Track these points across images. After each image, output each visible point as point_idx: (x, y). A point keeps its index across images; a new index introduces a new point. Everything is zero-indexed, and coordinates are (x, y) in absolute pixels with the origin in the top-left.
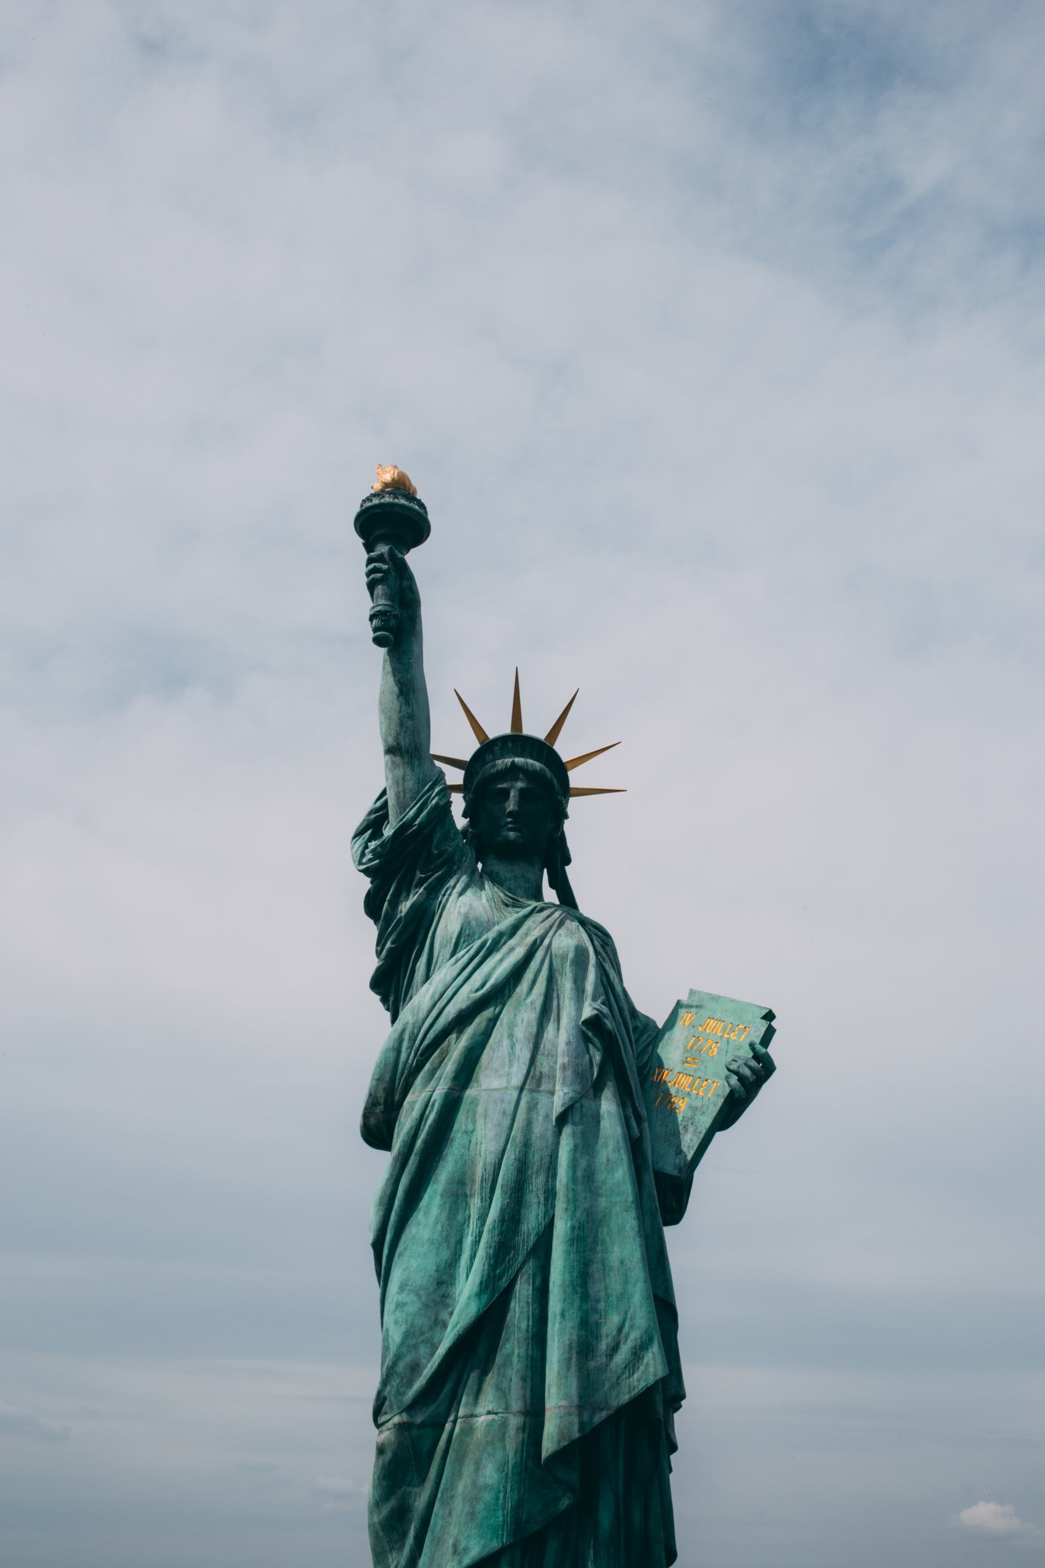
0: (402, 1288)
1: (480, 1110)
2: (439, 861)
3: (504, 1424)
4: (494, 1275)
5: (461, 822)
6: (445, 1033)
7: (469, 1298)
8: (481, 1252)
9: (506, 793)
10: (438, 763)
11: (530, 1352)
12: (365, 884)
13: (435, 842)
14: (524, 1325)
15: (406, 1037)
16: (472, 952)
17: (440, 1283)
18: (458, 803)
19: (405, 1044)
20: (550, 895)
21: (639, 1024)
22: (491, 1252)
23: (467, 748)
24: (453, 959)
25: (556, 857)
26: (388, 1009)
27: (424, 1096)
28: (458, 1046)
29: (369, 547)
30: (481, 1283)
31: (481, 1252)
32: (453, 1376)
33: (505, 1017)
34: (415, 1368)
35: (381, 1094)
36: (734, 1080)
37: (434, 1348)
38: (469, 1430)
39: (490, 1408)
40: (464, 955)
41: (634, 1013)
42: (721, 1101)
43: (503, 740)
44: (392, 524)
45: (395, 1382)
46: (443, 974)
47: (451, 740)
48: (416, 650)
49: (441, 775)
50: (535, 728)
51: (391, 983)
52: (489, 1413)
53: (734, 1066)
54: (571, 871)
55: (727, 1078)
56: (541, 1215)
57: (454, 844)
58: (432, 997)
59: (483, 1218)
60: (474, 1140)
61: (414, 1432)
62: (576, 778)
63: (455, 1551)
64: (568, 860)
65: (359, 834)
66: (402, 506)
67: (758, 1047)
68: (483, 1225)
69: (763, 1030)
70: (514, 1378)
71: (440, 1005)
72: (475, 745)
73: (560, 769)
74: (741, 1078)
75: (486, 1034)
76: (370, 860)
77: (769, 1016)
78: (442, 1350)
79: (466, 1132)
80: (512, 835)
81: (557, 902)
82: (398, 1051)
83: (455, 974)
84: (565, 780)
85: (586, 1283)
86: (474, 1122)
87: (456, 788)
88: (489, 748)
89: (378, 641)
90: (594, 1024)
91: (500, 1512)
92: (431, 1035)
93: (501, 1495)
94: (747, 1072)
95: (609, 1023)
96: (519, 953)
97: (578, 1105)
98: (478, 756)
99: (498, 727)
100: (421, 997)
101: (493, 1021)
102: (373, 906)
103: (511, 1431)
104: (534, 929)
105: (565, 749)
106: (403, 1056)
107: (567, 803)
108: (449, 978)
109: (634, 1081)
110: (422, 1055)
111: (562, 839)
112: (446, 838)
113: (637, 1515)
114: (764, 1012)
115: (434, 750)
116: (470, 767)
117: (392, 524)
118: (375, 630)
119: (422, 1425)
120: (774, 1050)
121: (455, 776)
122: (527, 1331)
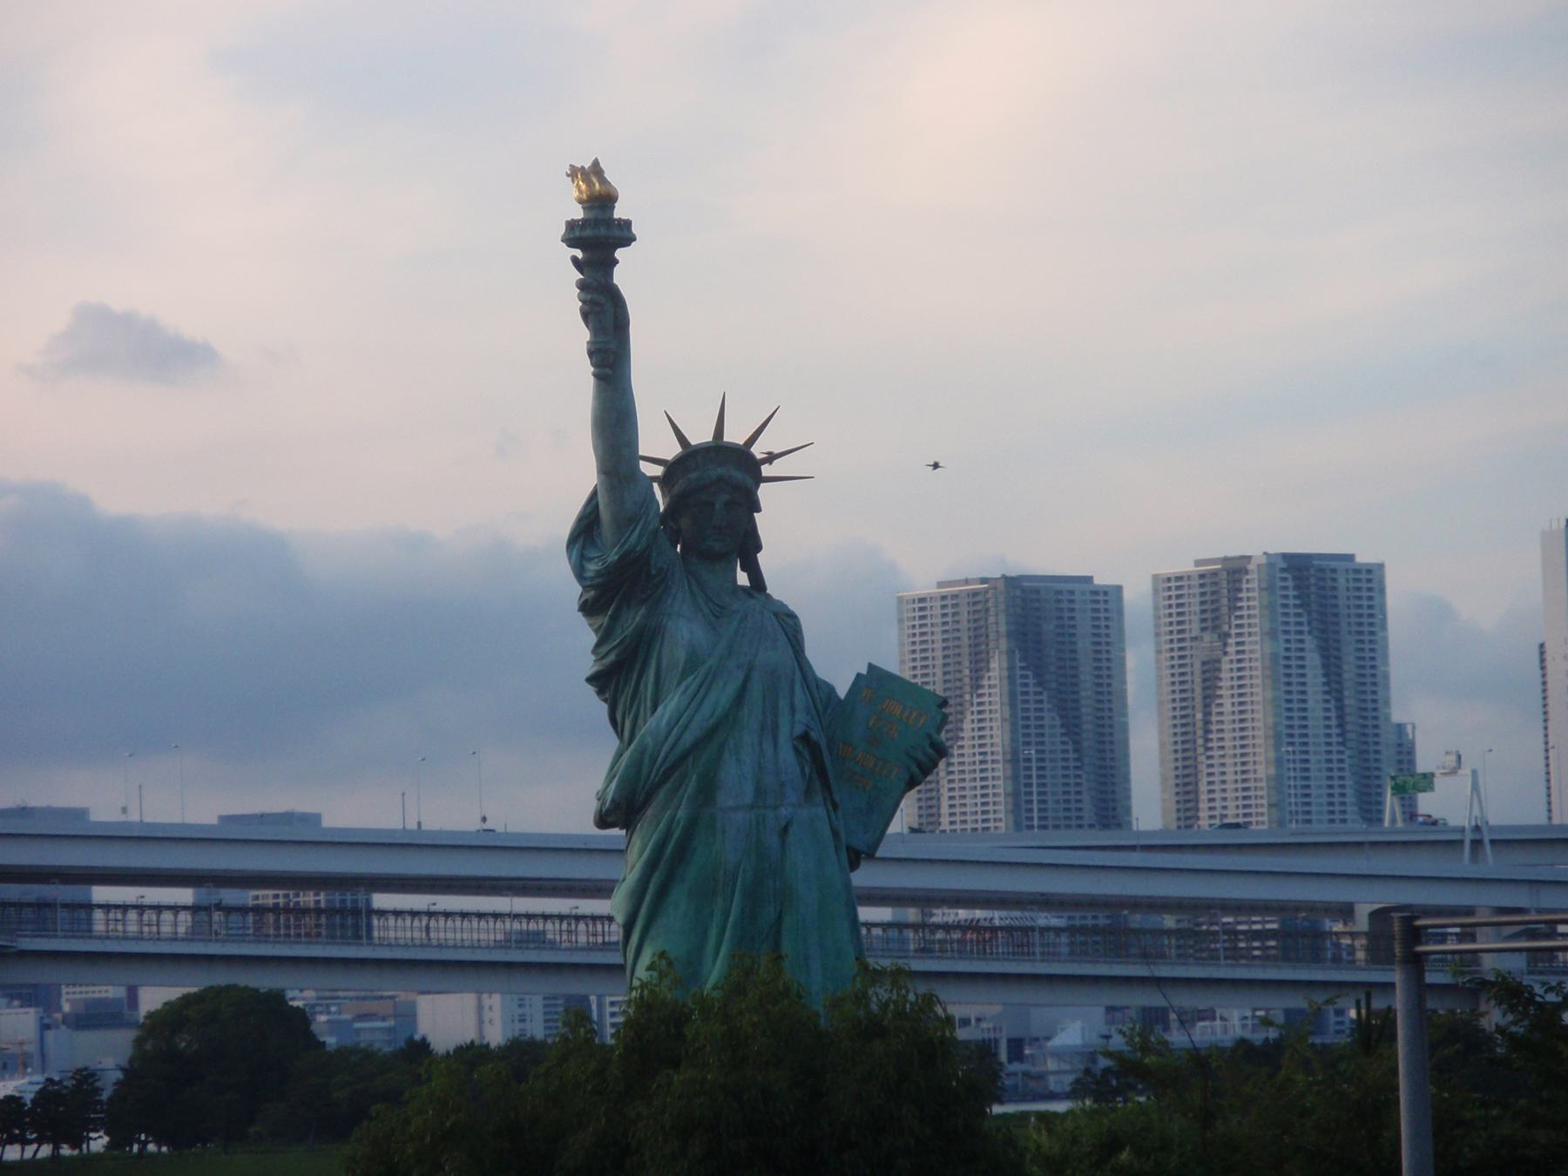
6: (684, 757)
20: (742, 579)
23: (672, 450)
24: (682, 687)
25: (748, 546)
26: (605, 701)
44: (598, 237)
59: (726, 914)
64: (759, 548)
87: (654, 479)
88: (691, 457)
90: (805, 738)
92: (672, 758)
95: (813, 735)
106: (644, 772)
116: (674, 469)
117: (598, 237)
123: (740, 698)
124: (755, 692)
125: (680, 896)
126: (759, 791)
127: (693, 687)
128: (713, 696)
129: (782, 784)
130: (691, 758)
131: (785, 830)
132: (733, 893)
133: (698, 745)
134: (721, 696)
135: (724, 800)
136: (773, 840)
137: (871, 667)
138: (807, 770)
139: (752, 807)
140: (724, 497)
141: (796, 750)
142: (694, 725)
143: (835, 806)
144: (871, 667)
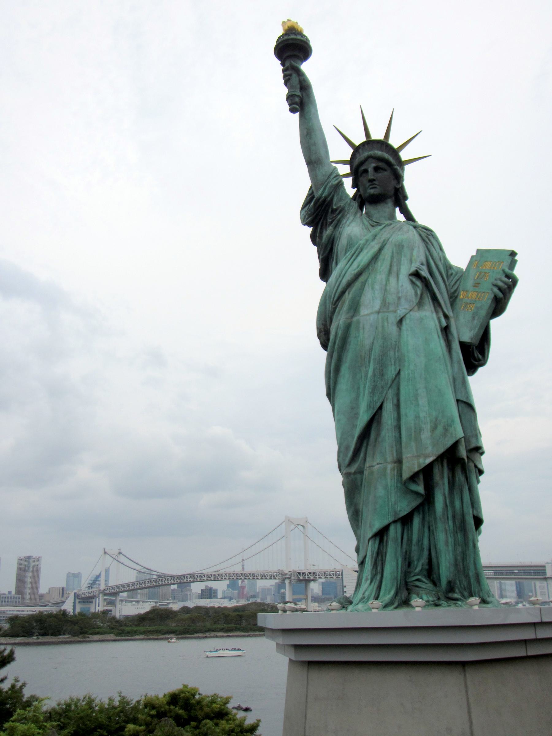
0: (338, 413)
1: (361, 325)
2: (337, 212)
3: (385, 469)
4: (373, 401)
5: (351, 192)
6: (343, 293)
7: (363, 413)
8: (367, 392)
9: (366, 171)
10: (334, 165)
11: (394, 434)
12: (310, 230)
13: (334, 202)
14: (389, 422)
15: (327, 298)
16: (353, 252)
17: (353, 408)
18: (348, 183)
19: (328, 302)
20: (400, 217)
21: (453, 272)
22: (371, 390)
23: (347, 153)
25: (399, 198)
27: (337, 323)
28: (348, 297)
29: (283, 64)
30: (367, 406)
31: (367, 392)
32: (363, 449)
33: (370, 280)
34: (347, 448)
35: (322, 327)
36: (496, 290)
37: (353, 437)
38: (372, 473)
39: (378, 461)
40: (349, 254)
41: (448, 267)
42: (490, 301)
43: (363, 144)
45: (341, 456)
46: (341, 265)
47: (339, 152)
48: (313, 110)
49: (335, 168)
50: (377, 135)
51: (325, 274)
52: (378, 464)
53: (495, 282)
54: (408, 203)
55: (492, 290)
56: (393, 370)
57: (344, 202)
58: (336, 277)
59: (366, 375)
60: (359, 340)
61: (352, 476)
62: (404, 155)
63: (370, 527)
64: (406, 198)
65: (303, 208)
66: (292, 39)
67: (507, 270)
68: (367, 379)
69: (510, 261)
70: (387, 448)
71: (340, 280)
72: (351, 151)
73: (395, 153)
74: (500, 289)
75: (362, 289)
76: (307, 219)
77: (513, 254)
78: (355, 439)
79: (356, 337)
80: (372, 191)
81: (405, 220)
82: (326, 306)
83: (345, 264)
84: (398, 158)
85: (417, 399)
86: (359, 331)
88: (357, 150)
89: (293, 110)
90: (417, 274)
91: (387, 508)
93: (386, 500)
94: (500, 284)
96: (376, 248)
97: (408, 316)
98: (353, 156)
99: (359, 139)
100: (333, 278)
101: (364, 284)
102: (314, 238)
103: (389, 471)
104: (384, 235)
105: (394, 142)
106: (328, 307)
107: (403, 170)
108: (343, 266)
109: (443, 298)
110: (334, 305)
111: (402, 188)
112: (340, 200)
113: (457, 503)
114: (510, 253)
115: (332, 159)
116: (350, 163)
117: (292, 49)
118: (290, 105)
119: (355, 473)
120: (517, 272)
121: (345, 169)
122: (391, 425)
123: (375, 258)
124: (387, 253)
125: (345, 370)
126: (385, 303)
127: (349, 257)
128: (359, 258)
129: (399, 298)
130: (347, 293)
131: (400, 322)
132: (369, 362)
133: (349, 285)
134: (364, 258)
135: (364, 311)
136: (394, 329)
137: (478, 251)
138: (419, 292)
139: (379, 312)
140: (373, 165)
141: (412, 283)
142: (347, 274)
143: (446, 317)
144: (478, 251)
